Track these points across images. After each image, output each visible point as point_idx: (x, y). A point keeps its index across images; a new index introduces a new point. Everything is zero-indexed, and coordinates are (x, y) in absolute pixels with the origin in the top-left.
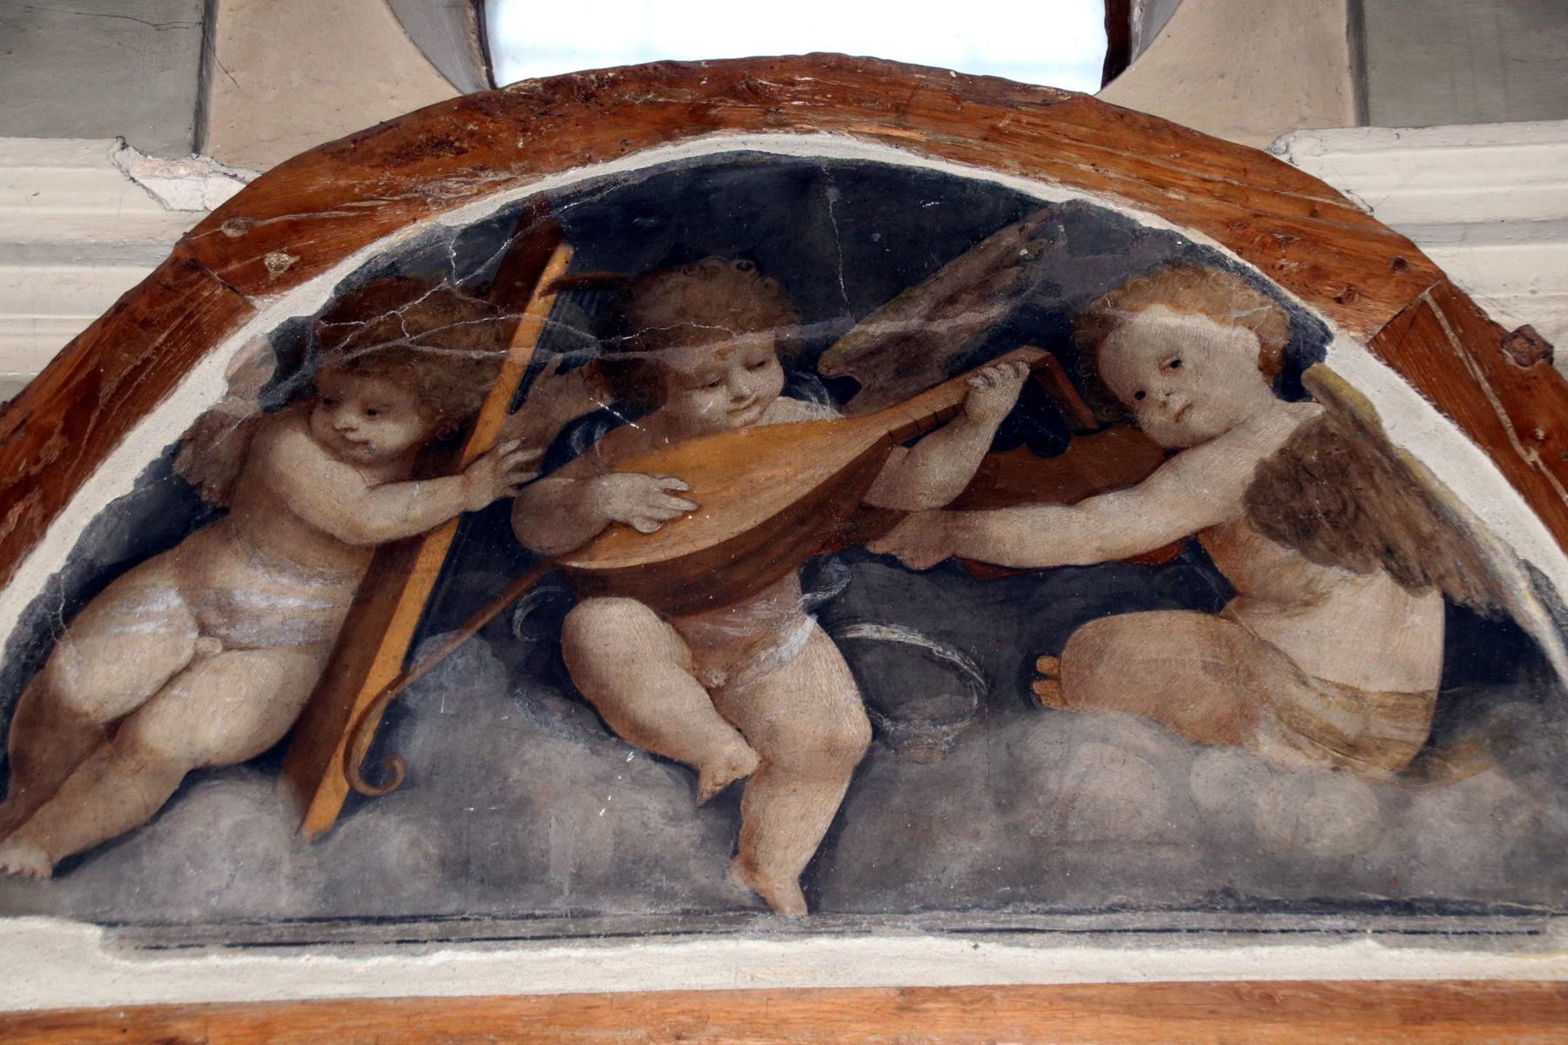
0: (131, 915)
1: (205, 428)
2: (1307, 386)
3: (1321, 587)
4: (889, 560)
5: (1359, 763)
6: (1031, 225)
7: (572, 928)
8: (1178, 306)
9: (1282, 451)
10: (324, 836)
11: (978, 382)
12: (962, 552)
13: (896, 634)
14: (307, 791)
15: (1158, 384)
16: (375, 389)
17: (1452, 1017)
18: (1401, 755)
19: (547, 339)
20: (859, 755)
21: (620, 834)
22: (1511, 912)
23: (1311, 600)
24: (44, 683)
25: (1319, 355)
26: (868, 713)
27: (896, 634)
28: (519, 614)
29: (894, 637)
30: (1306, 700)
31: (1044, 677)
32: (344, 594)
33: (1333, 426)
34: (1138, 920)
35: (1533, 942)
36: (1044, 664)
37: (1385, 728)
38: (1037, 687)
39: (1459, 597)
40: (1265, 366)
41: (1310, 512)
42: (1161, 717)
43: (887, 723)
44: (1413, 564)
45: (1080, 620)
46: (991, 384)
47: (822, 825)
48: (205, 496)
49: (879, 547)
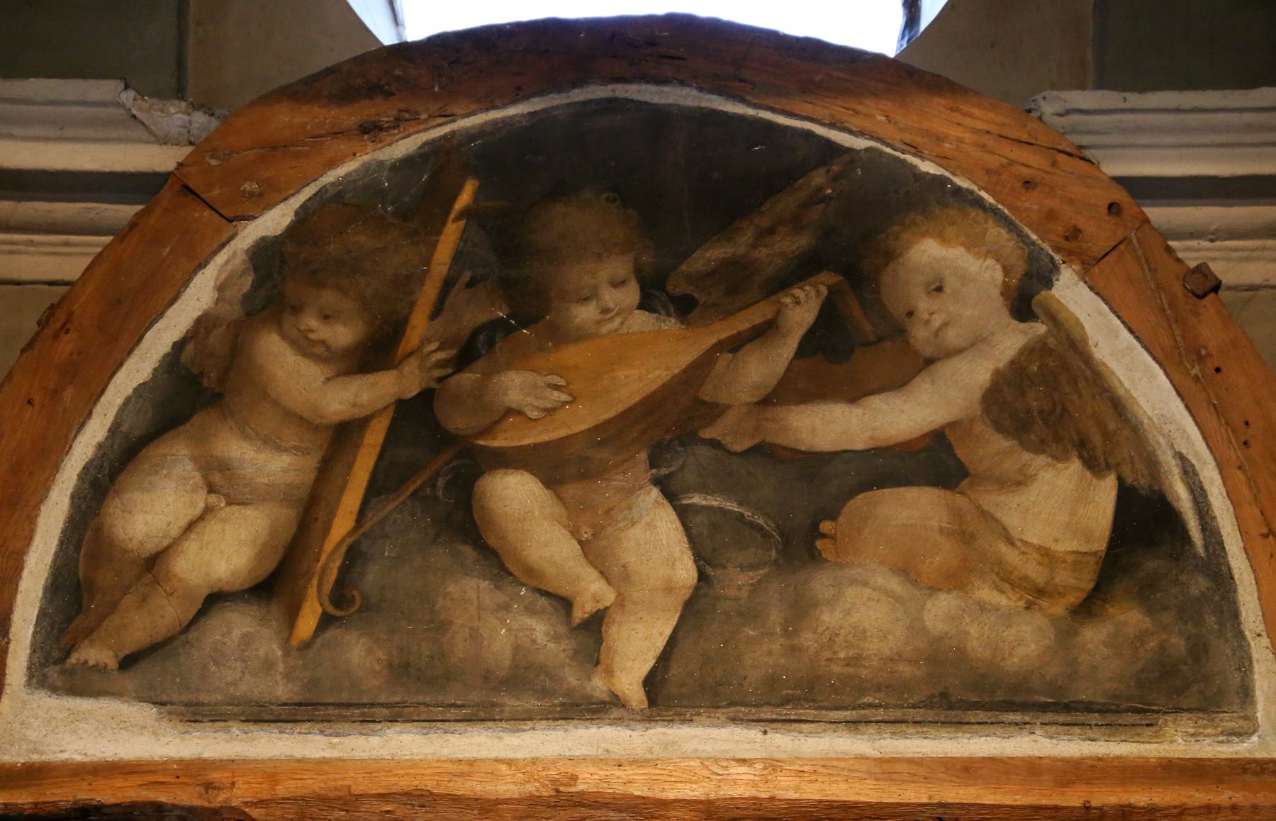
0: (175, 698)
1: (203, 325)
2: (1036, 309)
3: (1031, 471)
4: (715, 444)
6: (835, 168)
7: (482, 714)
8: (943, 240)
9: (1012, 362)
10: (306, 645)
11: (788, 300)
12: (770, 439)
13: (714, 502)
14: (292, 614)
15: (924, 305)
16: (329, 298)
17: (1088, 782)
18: (1073, 598)
19: (458, 257)
20: (686, 594)
21: (516, 648)
23: (1020, 481)
24: (99, 530)
25: (1048, 283)
26: (696, 561)
27: (714, 502)
28: (441, 482)
29: (715, 504)
30: (1011, 556)
31: (824, 536)
32: (312, 461)
33: (1051, 341)
34: (881, 714)
35: (1148, 732)
36: (826, 526)
37: (1064, 577)
38: (819, 544)
40: (1006, 291)
41: (1029, 411)
42: (905, 570)
43: (709, 570)
45: (853, 493)
46: (797, 302)
47: (661, 643)
48: (205, 383)
49: (707, 434)
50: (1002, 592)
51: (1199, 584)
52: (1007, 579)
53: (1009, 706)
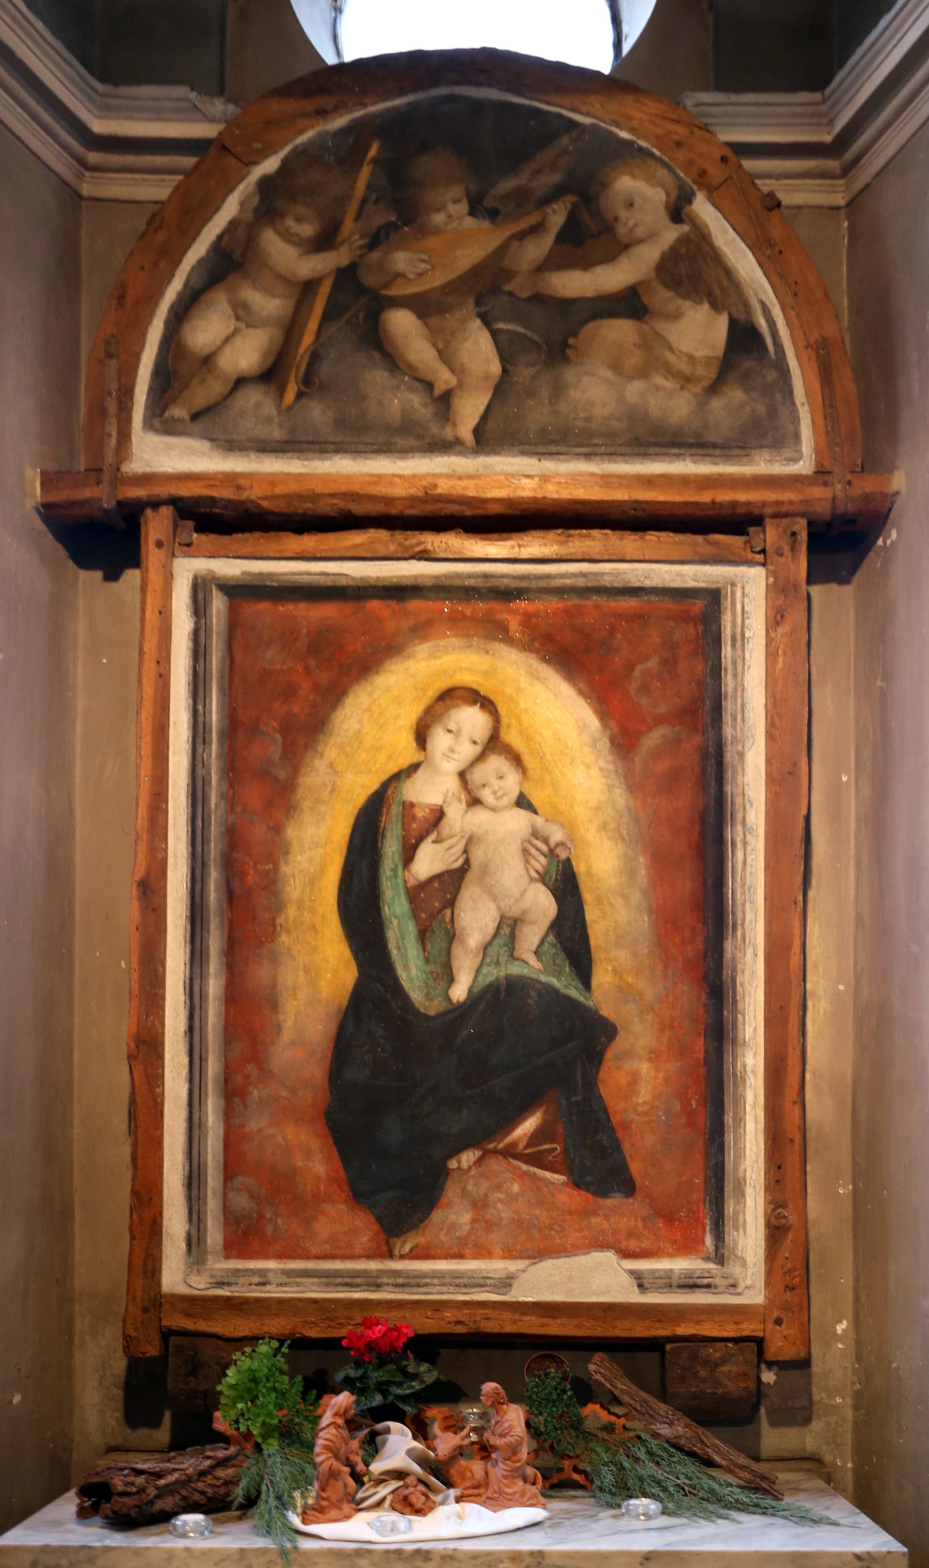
5: (690, 386)
18: (706, 383)
22: (739, 447)
30: (672, 359)
35: (746, 459)
37: (700, 371)
39: (735, 315)
44: (719, 301)
50: (667, 379)
51: (772, 375)
52: (670, 372)
53: (672, 445)
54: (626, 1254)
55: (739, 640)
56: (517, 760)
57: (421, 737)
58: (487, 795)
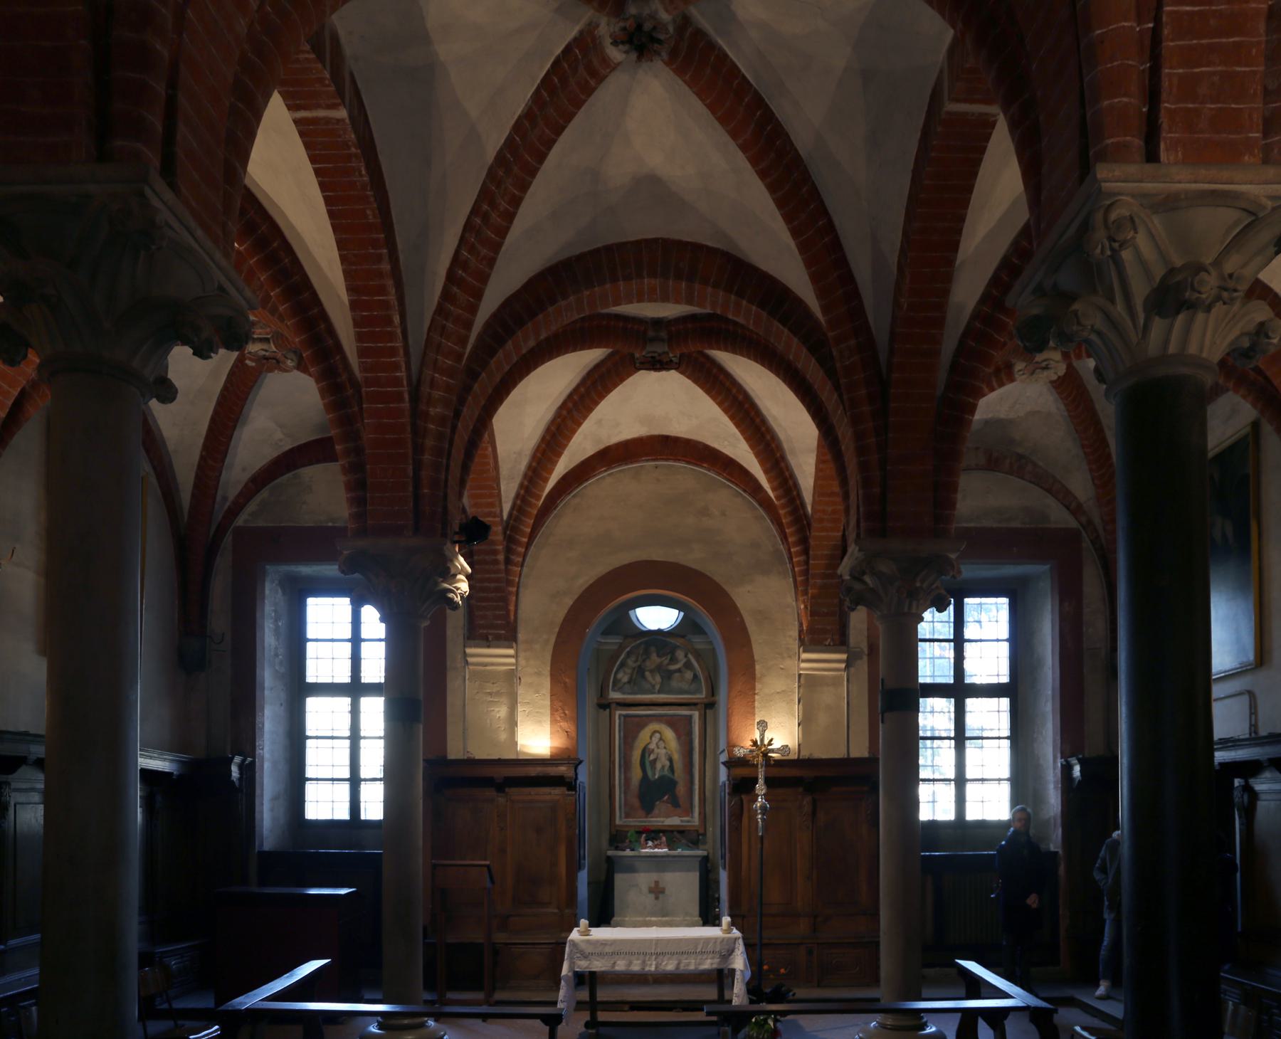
54: (680, 817)
55: (694, 723)
56: (664, 741)
57: (651, 738)
58: (660, 747)
